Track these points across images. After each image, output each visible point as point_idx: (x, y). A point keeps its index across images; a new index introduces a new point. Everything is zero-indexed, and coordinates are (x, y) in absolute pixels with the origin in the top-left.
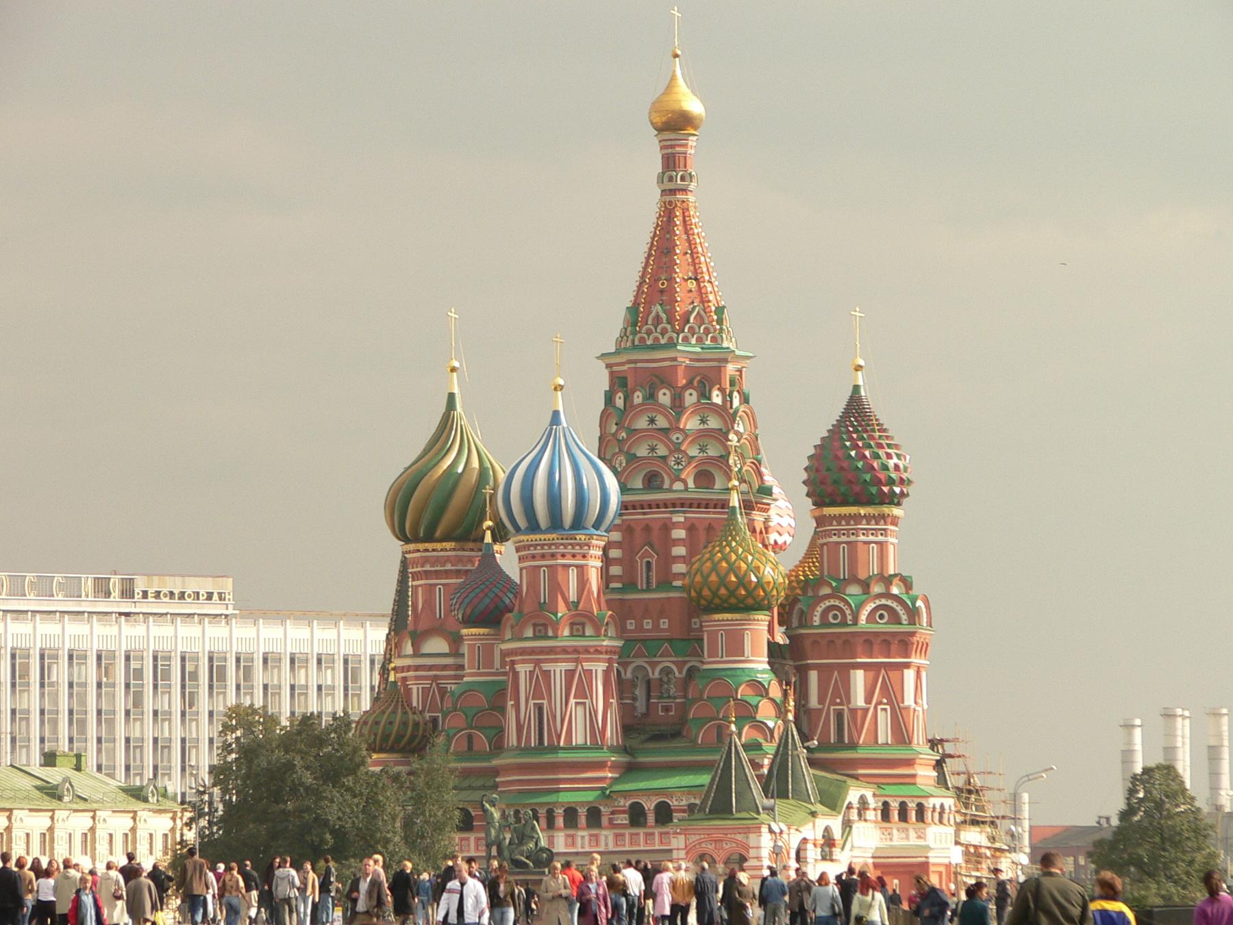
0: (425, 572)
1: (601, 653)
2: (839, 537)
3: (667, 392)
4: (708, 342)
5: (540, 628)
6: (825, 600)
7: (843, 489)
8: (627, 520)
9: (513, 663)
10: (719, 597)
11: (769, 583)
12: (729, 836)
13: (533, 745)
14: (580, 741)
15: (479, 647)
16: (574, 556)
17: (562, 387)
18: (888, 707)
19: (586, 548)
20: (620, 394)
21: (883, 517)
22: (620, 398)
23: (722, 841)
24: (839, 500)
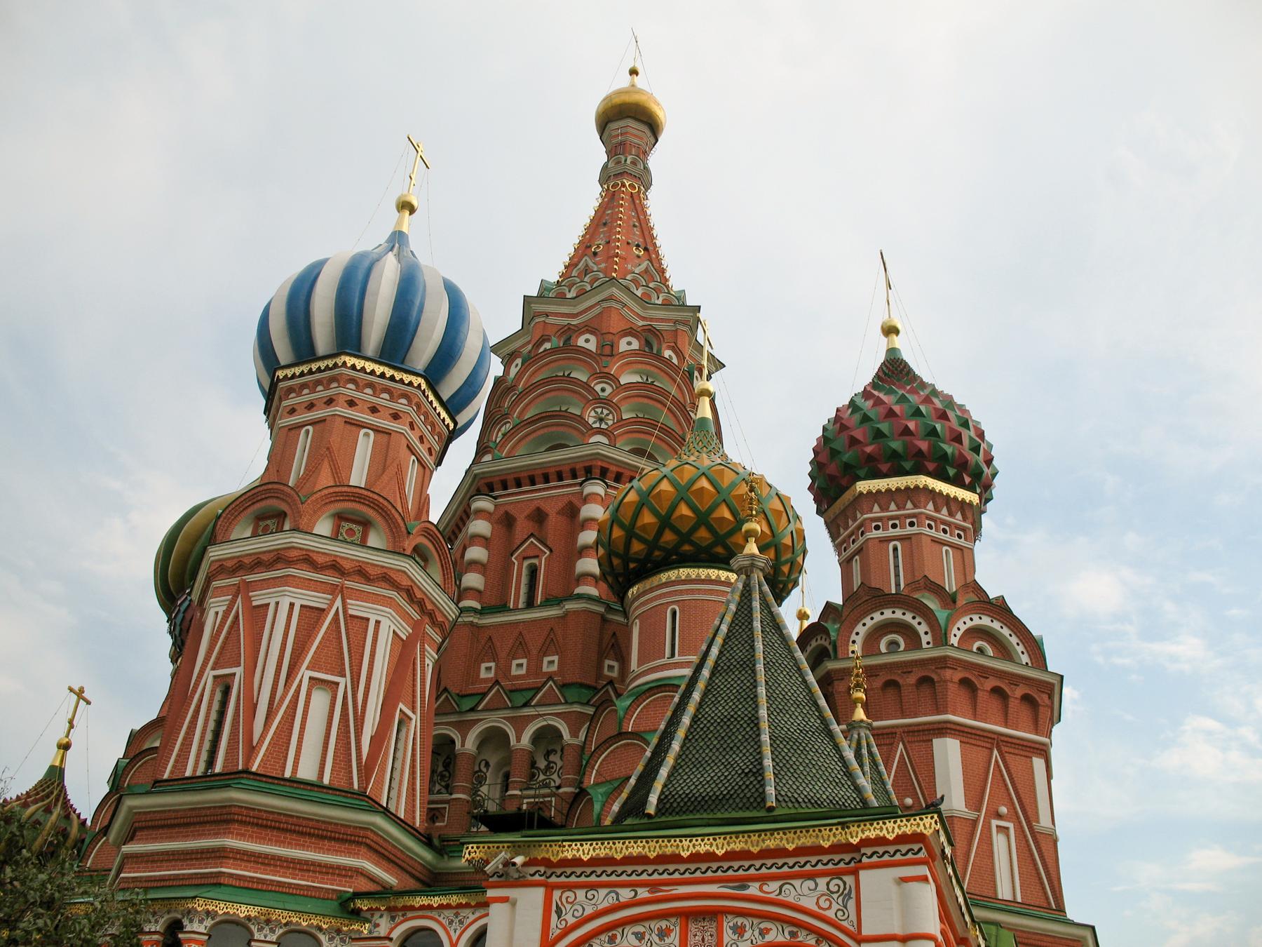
1: (395, 586)
3: (593, 339)
4: (660, 302)
5: (269, 522)
6: (874, 610)
7: (896, 445)
9: (203, 611)
10: (675, 530)
11: (778, 513)
12: (753, 889)
13: (188, 773)
14: (307, 771)
16: (374, 410)
17: (412, 210)
18: (1011, 825)
19: (404, 401)
20: (519, 361)
21: (963, 506)
22: (517, 365)
23: (714, 915)
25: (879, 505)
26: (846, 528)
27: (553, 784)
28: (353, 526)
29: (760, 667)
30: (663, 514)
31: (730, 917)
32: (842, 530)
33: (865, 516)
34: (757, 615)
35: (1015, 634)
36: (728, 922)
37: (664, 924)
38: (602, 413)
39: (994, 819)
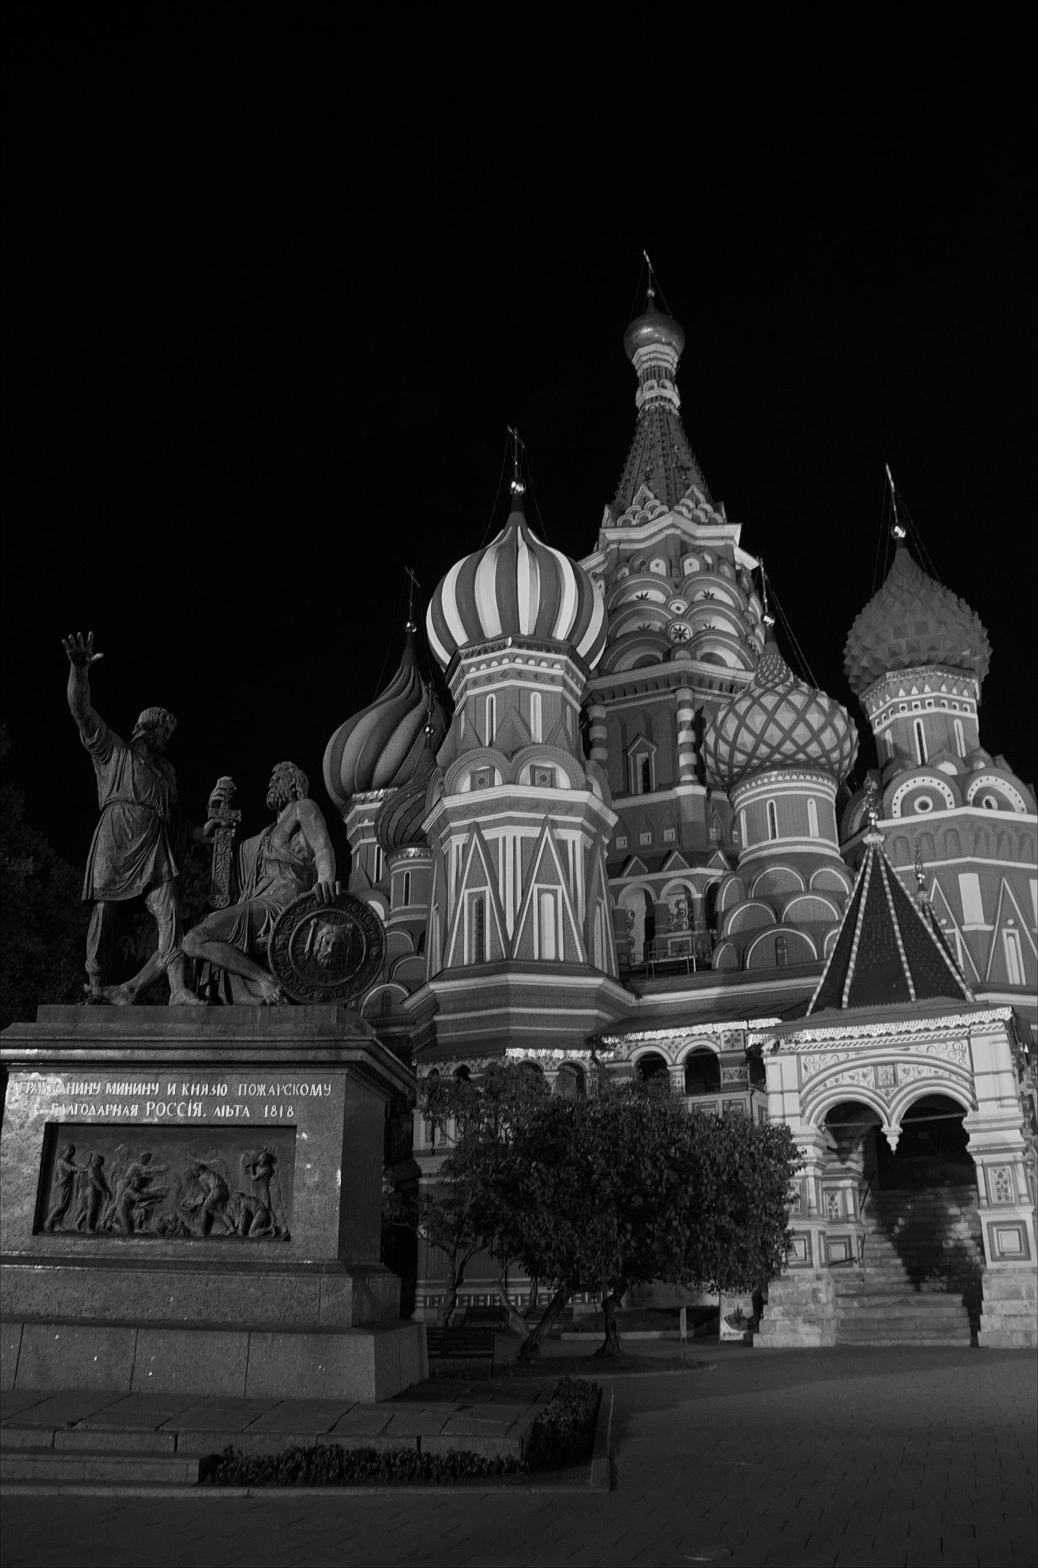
0: (363, 829)
2: (910, 709)
3: (662, 564)
4: (707, 521)
6: (907, 779)
8: (612, 712)
9: (442, 842)
12: (913, 1050)
13: (466, 962)
14: (549, 954)
15: (408, 875)
16: (537, 677)
18: (1016, 932)
19: (557, 666)
20: (602, 583)
22: (600, 587)
23: (893, 1063)
24: (906, 661)
25: (904, 690)
26: (878, 708)
27: (684, 927)
28: (543, 773)
29: (893, 912)
30: (758, 733)
31: (901, 1064)
32: (874, 709)
33: (895, 700)
34: (884, 875)
35: (1015, 787)
36: (900, 1067)
37: (865, 1070)
38: (680, 629)
39: (1005, 927)
